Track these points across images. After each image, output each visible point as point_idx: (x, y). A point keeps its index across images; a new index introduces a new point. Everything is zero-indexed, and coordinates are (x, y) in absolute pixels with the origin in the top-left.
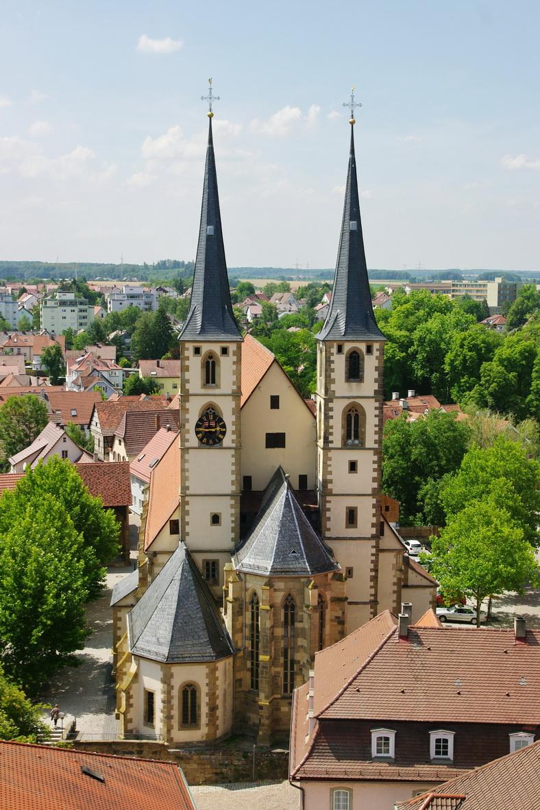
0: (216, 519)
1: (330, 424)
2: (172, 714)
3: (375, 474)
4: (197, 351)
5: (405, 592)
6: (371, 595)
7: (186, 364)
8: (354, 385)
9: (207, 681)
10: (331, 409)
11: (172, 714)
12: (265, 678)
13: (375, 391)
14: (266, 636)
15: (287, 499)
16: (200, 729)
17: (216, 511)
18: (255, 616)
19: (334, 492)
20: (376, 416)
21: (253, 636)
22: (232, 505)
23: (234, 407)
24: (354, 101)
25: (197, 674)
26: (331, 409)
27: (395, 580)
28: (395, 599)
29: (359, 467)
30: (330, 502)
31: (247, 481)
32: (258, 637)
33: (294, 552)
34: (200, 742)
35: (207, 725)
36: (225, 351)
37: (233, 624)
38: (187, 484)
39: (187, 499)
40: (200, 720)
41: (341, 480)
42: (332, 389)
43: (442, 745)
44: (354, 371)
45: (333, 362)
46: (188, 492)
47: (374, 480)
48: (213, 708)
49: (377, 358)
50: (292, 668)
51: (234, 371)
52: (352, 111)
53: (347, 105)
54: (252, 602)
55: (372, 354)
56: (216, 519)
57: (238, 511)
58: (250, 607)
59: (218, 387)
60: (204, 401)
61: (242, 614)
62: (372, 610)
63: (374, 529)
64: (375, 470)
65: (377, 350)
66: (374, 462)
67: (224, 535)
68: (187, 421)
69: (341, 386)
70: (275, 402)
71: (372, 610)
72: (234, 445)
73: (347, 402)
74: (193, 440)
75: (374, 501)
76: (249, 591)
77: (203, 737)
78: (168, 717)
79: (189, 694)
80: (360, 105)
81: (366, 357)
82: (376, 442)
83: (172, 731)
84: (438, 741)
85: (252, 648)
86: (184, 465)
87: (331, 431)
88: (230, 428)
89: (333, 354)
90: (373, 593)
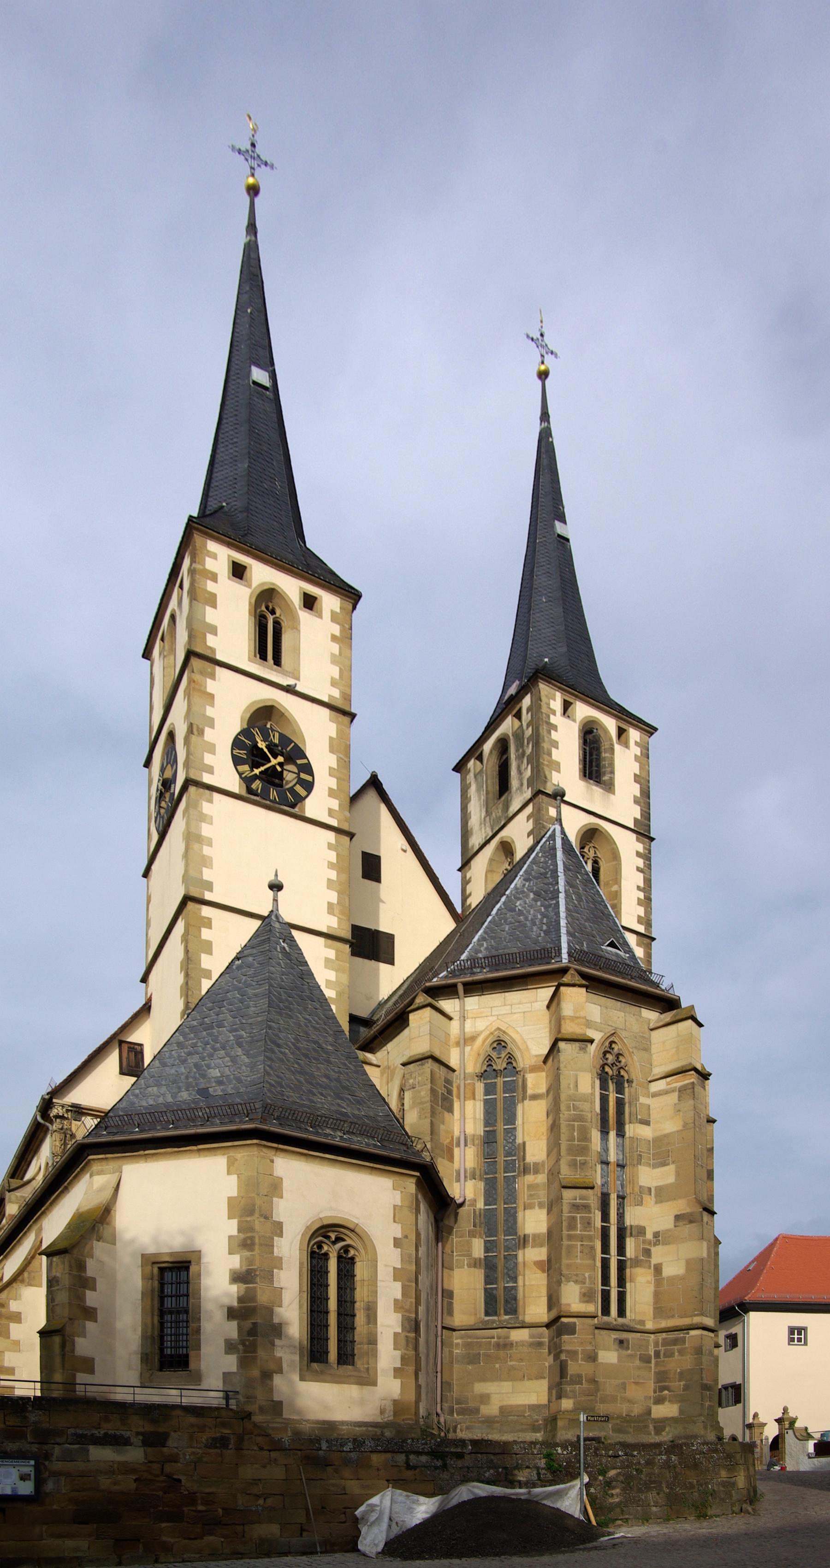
9: (397, 1231)
12: (582, 1238)
35: (398, 1372)
40: (374, 1354)
54: (488, 1073)
58: (480, 1087)
61: (450, 1110)
76: (479, 1041)
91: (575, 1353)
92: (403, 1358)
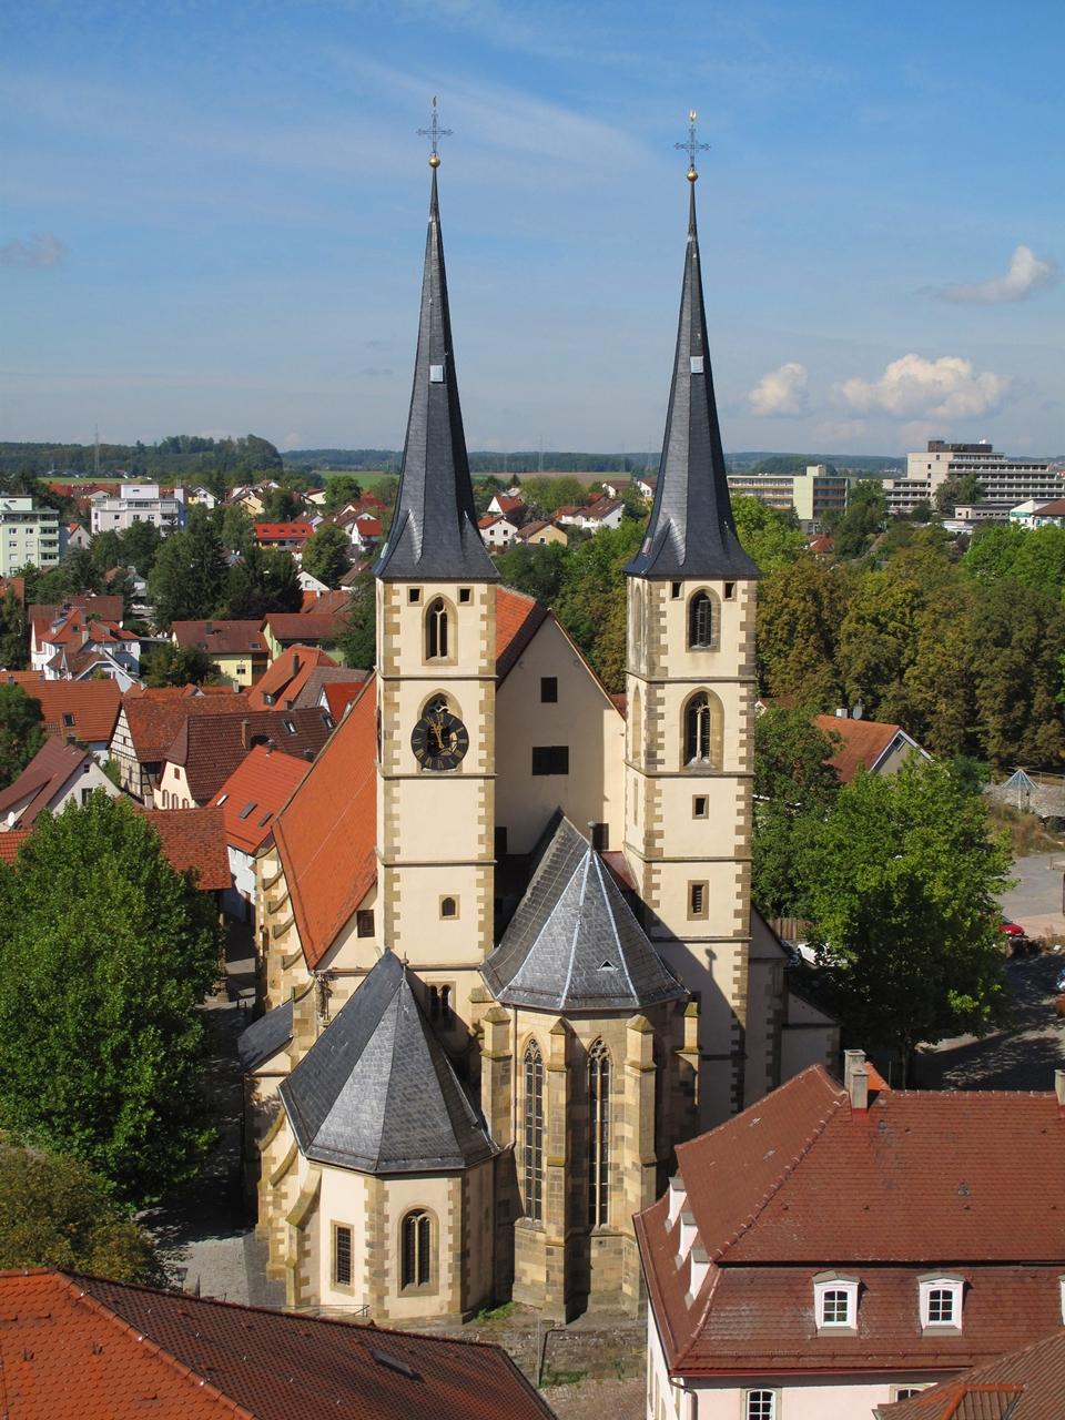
0: (449, 907)
1: (660, 729)
2: (386, 1267)
3: (741, 820)
4: (414, 595)
5: (787, 1035)
6: (734, 1042)
7: (395, 621)
8: (702, 656)
10: (661, 701)
11: (386, 1267)
12: (557, 1196)
13: (740, 667)
14: (560, 1120)
15: (592, 867)
16: (437, 1294)
17: (449, 893)
18: (535, 1085)
19: (666, 855)
20: (742, 713)
21: (529, 1120)
22: (478, 880)
23: (482, 698)
24: (696, 138)
25: (438, 1196)
26: (661, 701)
27: (770, 1014)
28: (770, 1049)
29: (712, 806)
30: (659, 872)
31: (500, 836)
32: (539, 1123)
33: (607, 965)
34: (437, 1318)
35: (450, 1286)
36: (465, 596)
37: (493, 1100)
38: (397, 842)
39: (396, 870)
41: (682, 832)
42: (662, 665)
43: (940, 1303)
44: (701, 630)
45: (664, 614)
46: (399, 859)
47: (739, 830)
48: (464, 1255)
49: (744, 606)
50: (604, 1178)
51: (482, 632)
52: (692, 158)
53: (683, 146)
55: (734, 600)
56: (449, 907)
57: (491, 891)
58: (524, 1067)
59: (454, 663)
60: (431, 688)
62: (736, 1070)
63: (740, 920)
64: (739, 812)
65: (744, 592)
66: (739, 798)
67: (468, 937)
68: (397, 725)
69: (679, 660)
70: (549, 690)
71: (736, 1070)
72: (482, 770)
73: (689, 689)
74: (407, 760)
75: (738, 868)
77: (442, 1309)
78: (378, 1275)
79: (415, 1227)
80: (706, 147)
81: (724, 605)
82: (742, 761)
83: (387, 1298)
84: (934, 1295)
85: (529, 1143)
86: (391, 810)
87: (660, 741)
88: (476, 737)
89: (663, 600)
90: (738, 1038)
91: (553, 1267)
92: (454, 1278)
